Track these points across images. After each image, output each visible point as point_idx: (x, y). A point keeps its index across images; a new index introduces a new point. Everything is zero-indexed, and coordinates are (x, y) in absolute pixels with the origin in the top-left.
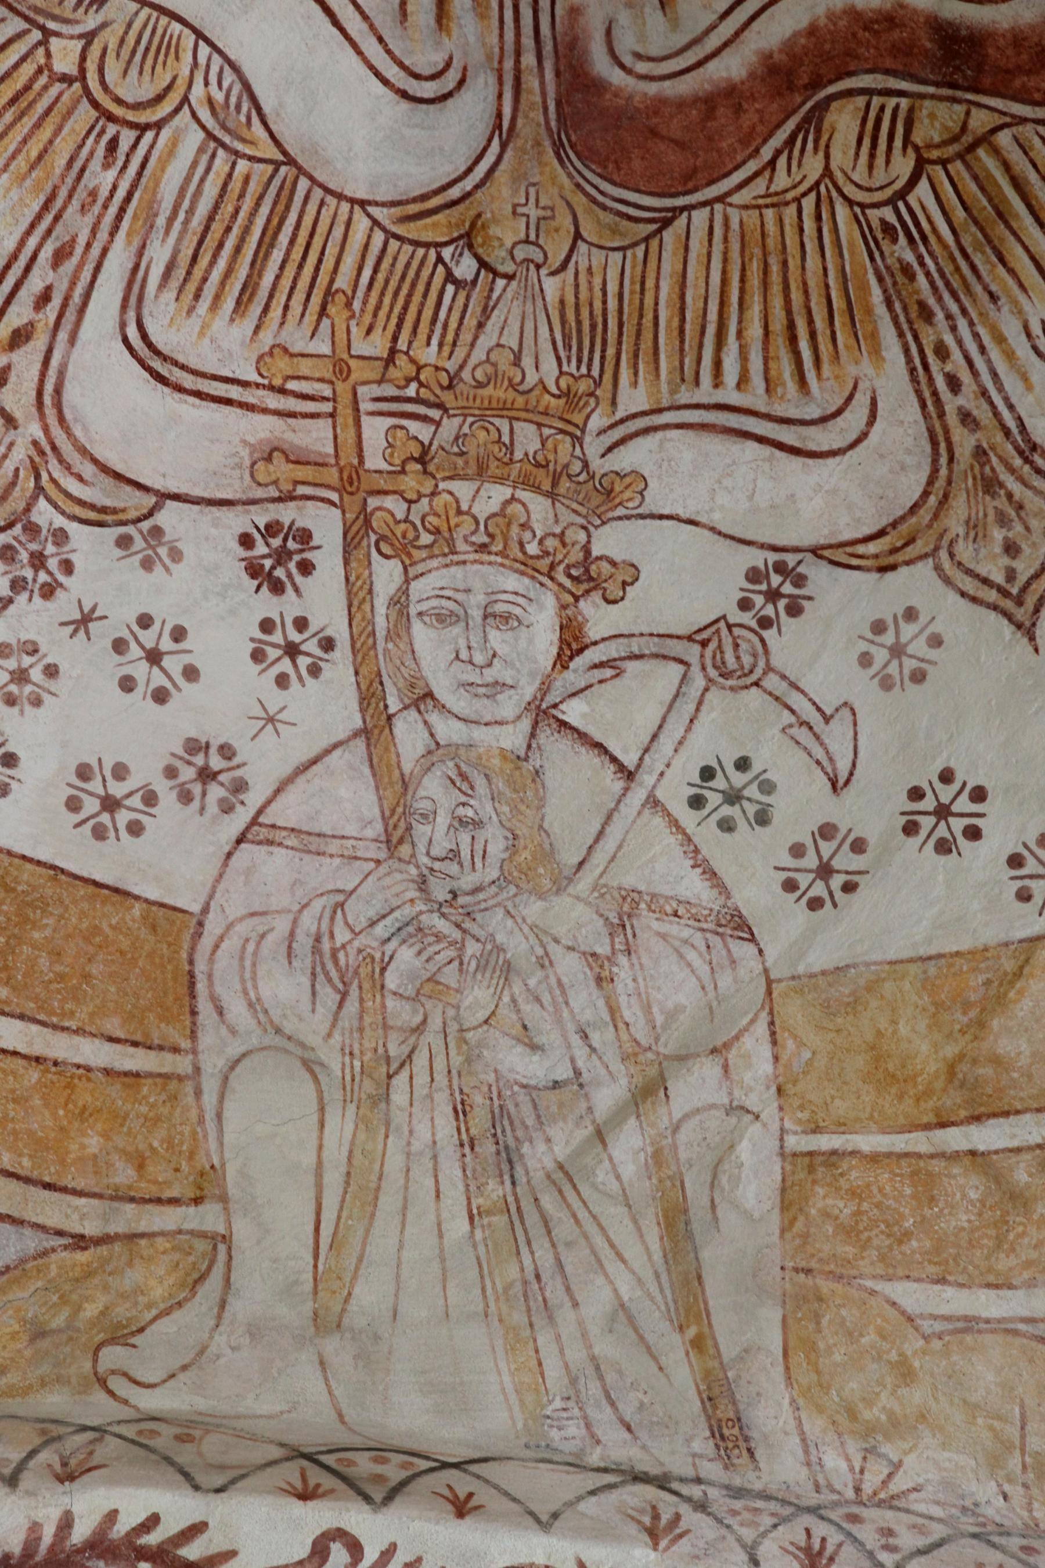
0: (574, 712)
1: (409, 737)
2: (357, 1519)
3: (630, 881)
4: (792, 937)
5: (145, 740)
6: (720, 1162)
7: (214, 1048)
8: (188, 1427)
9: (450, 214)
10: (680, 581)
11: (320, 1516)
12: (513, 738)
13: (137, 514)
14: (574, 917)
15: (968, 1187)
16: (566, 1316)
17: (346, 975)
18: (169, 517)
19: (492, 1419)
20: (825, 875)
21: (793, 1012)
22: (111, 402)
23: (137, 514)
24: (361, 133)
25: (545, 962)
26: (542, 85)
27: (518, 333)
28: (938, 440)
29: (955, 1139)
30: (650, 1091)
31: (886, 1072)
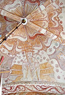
0: (33, 56)
1: (28, 58)
2: (26, 84)
3: (35, 62)
4: (40, 63)
5: (20, 60)
6: (38, 71)
7: (23, 69)
8: (22, 82)
9: (27, 41)
10: (36, 51)
11: (26, 84)
12: (31, 58)
13: (19, 53)
14: (33, 63)
15: (46, 70)
16: (33, 77)
17: (27, 66)
18: (20, 53)
19: (31, 80)
20: (41, 61)
21: (40, 65)
22: (17, 50)
23: (19, 53)
24: (23, 40)
25: (33, 65)
26: (29, 37)
27: (30, 44)
28: (43, 46)
29: (45, 69)
30: (36, 69)
31: (43, 67)
